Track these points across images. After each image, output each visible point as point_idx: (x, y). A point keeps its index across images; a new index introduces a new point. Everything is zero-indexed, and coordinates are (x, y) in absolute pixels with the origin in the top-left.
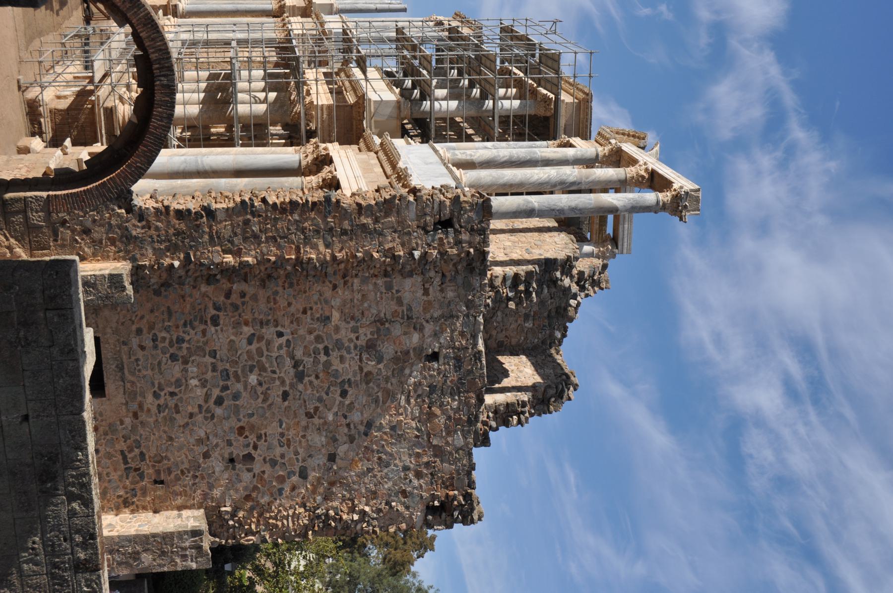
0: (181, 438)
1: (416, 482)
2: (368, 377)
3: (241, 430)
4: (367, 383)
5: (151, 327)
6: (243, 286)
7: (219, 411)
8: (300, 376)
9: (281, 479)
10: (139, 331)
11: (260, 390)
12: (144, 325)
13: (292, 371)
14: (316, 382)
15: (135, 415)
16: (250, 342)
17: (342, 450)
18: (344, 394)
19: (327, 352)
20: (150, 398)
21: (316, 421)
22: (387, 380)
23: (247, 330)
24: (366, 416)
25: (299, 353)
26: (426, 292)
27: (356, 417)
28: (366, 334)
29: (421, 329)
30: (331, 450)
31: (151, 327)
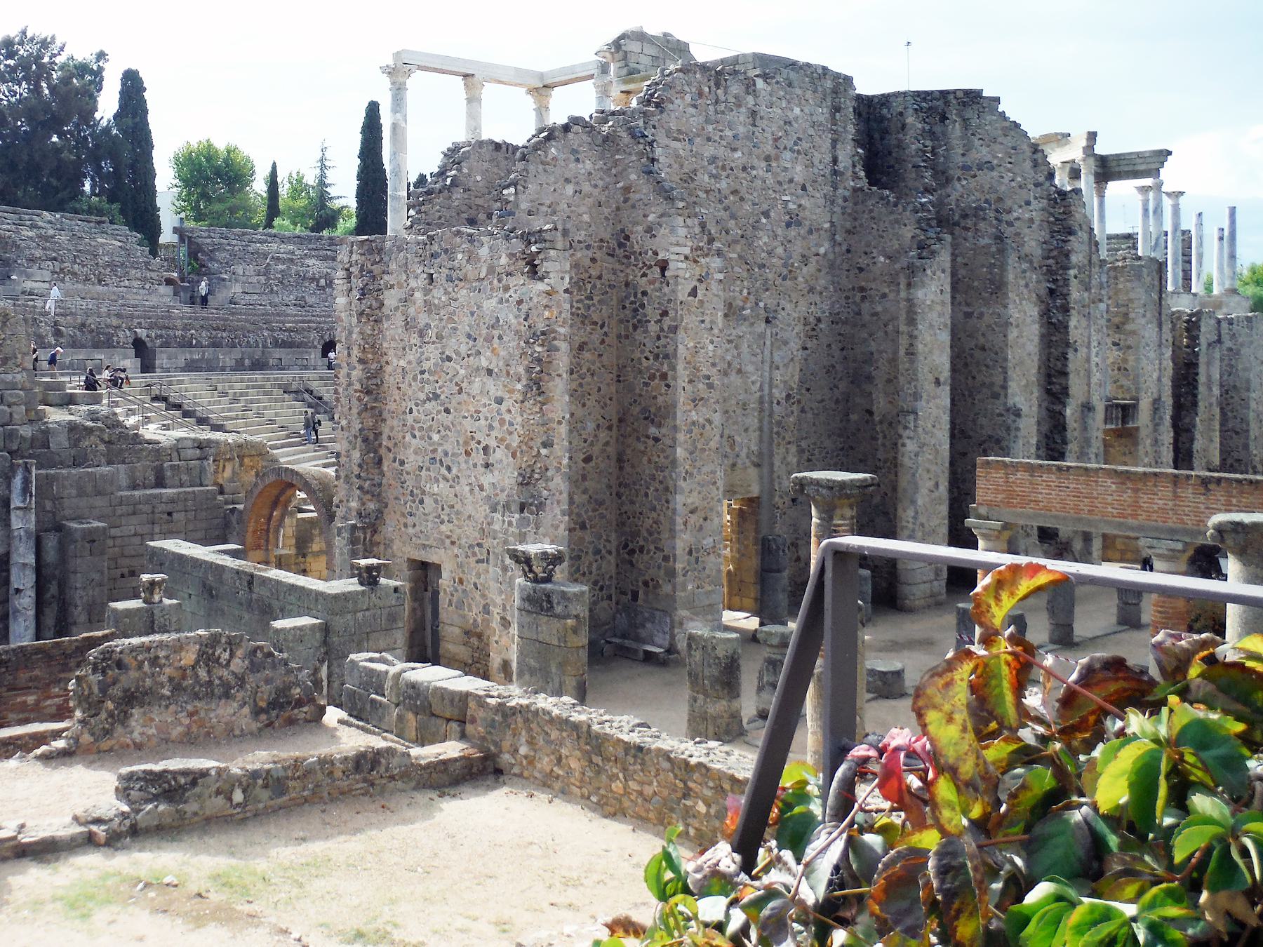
0: (469, 509)
1: (511, 292)
2: (440, 337)
3: (468, 454)
4: (442, 338)
5: (403, 515)
6: (385, 436)
7: (454, 471)
8: (436, 397)
9: (502, 422)
10: (406, 526)
11: (443, 433)
12: (402, 520)
13: (433, 402)
14: (440, 383)
15: (453, 543)
16: (414, 437)
17: (484, 363)
18: (449, 359)
19: (422, 372)
20: (443, 528)
21: (464, 385)
22: (441, 320)
23: (408, 437)
24: (464, 339)
25: (422, 396)
26: (392, 287)
27: (463, 349)
28: (415, 339)
29: (413, 290)
30: (483, 373)
31: (403, 515)
